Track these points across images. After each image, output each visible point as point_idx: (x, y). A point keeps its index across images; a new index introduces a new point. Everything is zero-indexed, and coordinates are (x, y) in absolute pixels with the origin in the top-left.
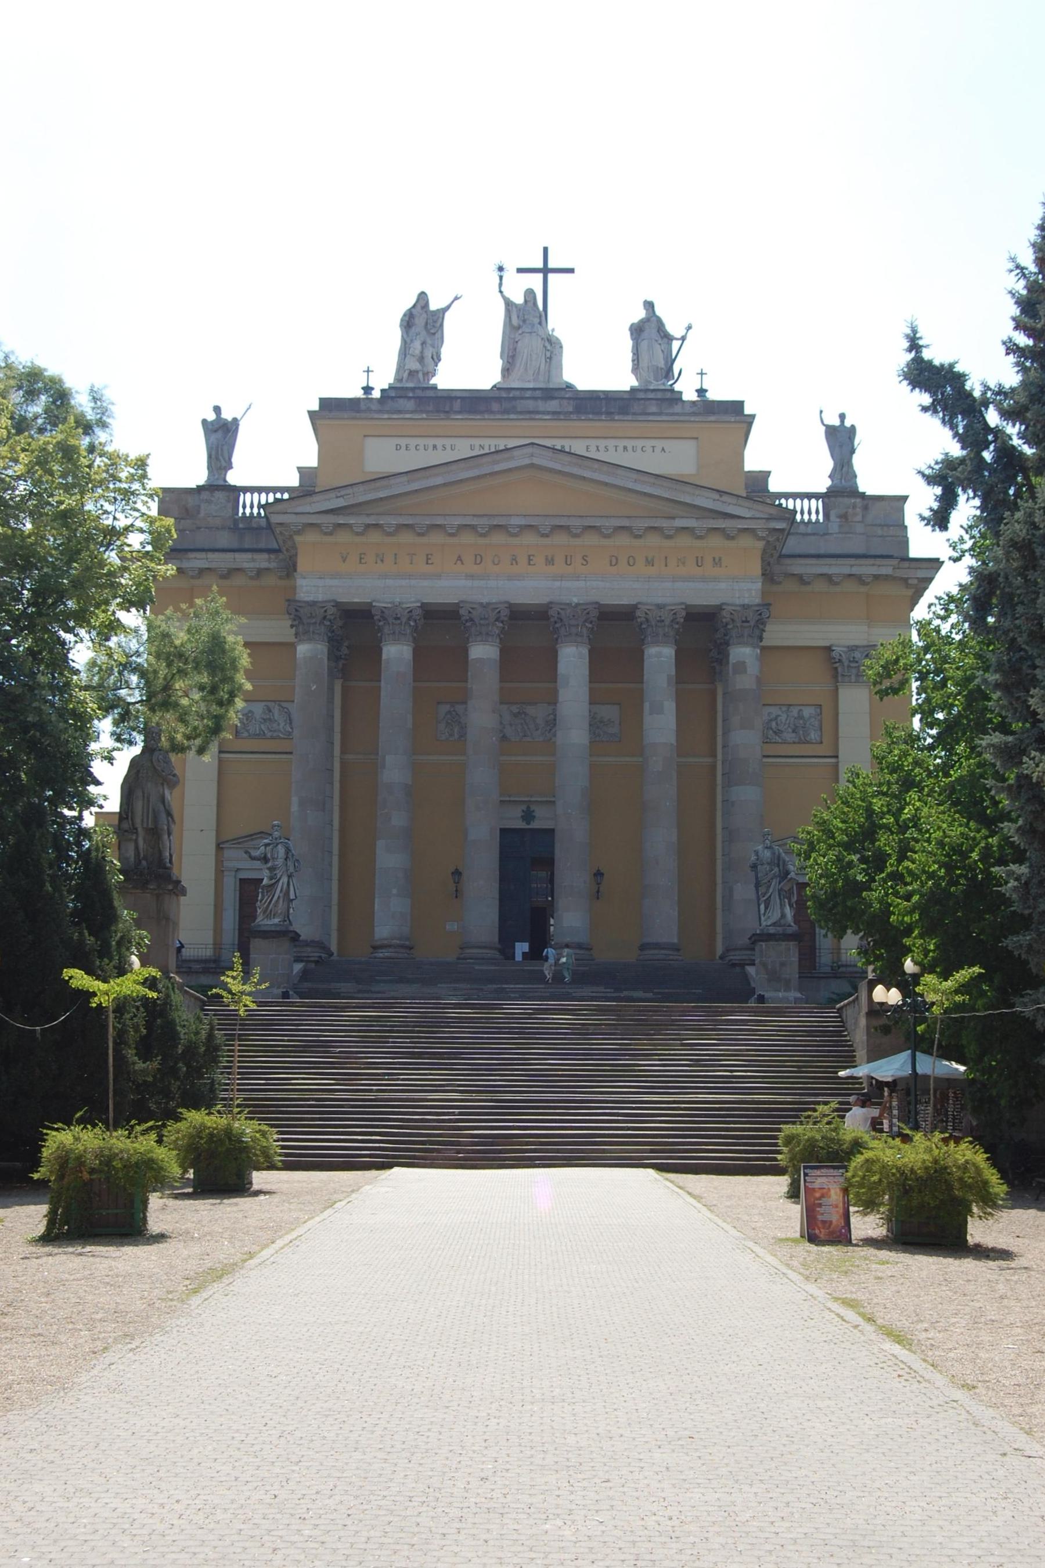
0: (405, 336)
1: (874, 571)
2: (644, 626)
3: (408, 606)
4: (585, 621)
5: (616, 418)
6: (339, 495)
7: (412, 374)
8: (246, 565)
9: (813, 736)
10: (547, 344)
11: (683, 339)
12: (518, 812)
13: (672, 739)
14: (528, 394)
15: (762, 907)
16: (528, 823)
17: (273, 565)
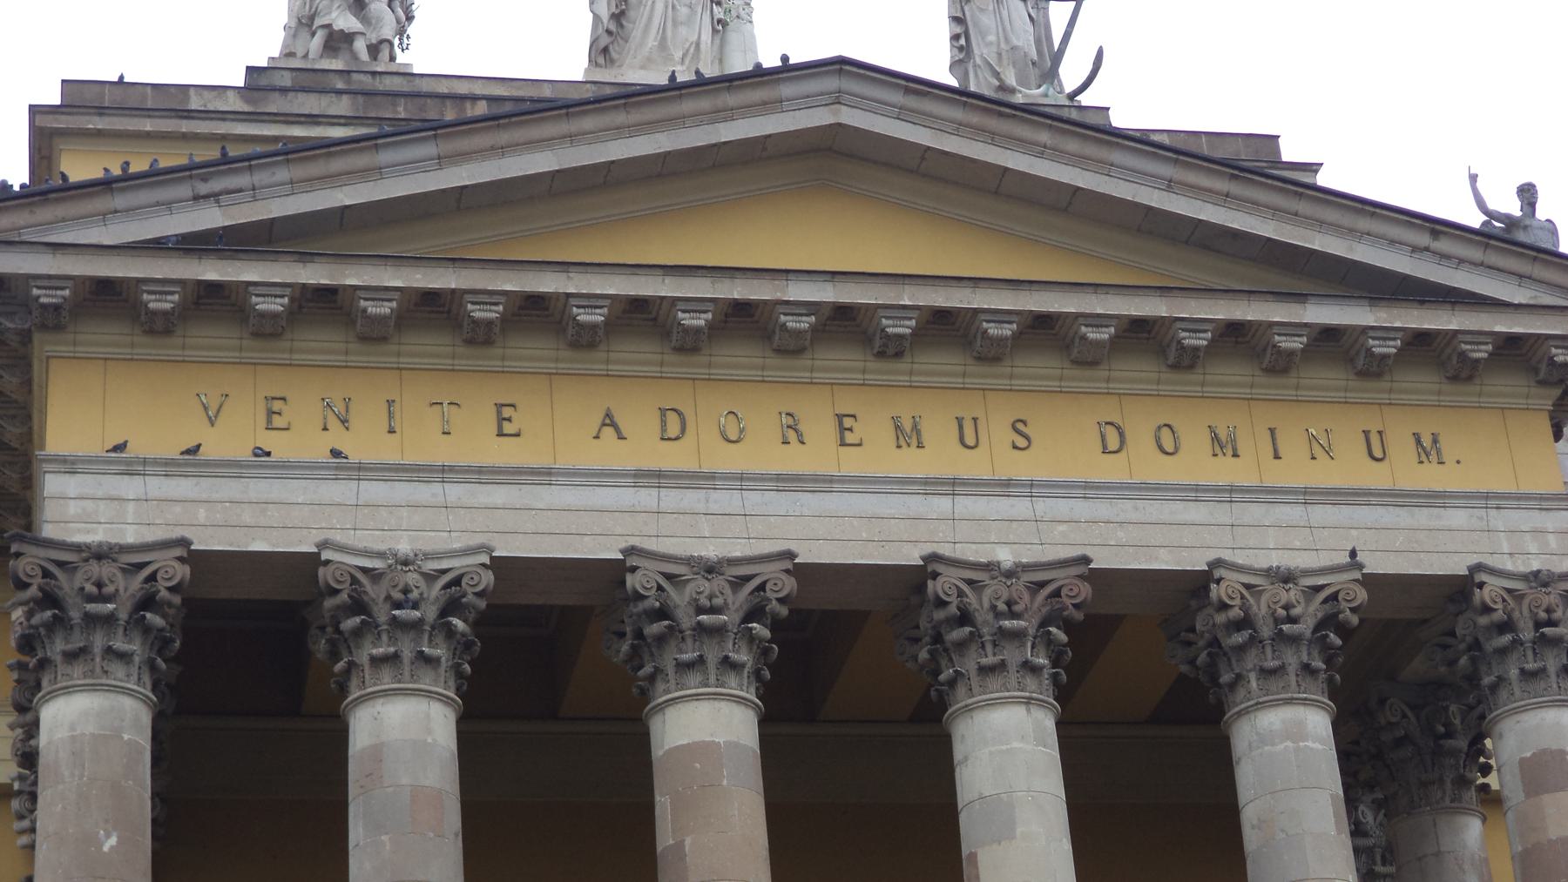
3: (444, 565)
6: (203, 188)
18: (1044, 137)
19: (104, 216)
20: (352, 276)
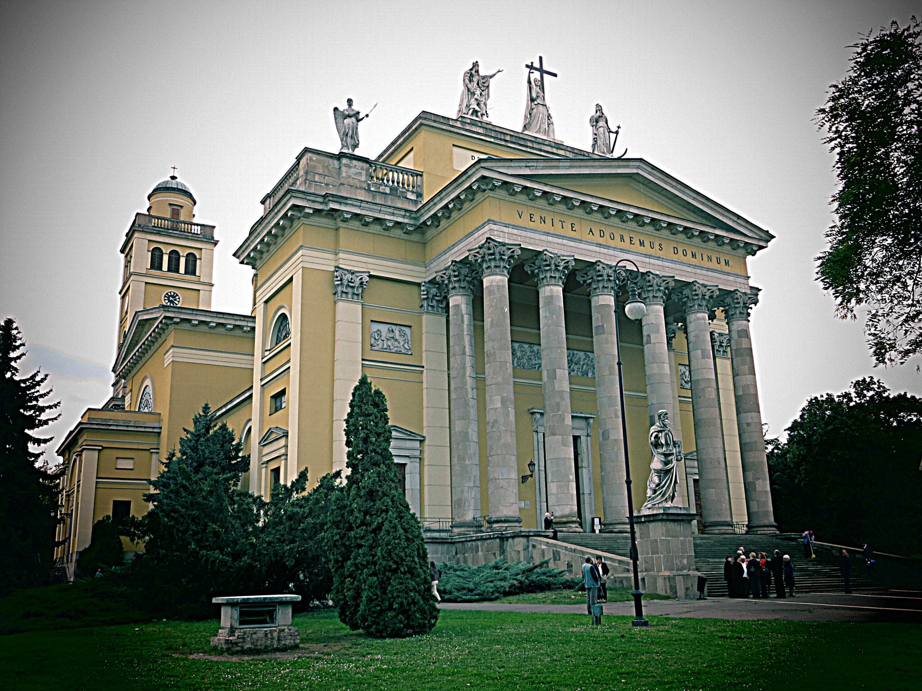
6: (528, 165)
11: (617, 133)
18: (674, 184)
19: (509, 167)
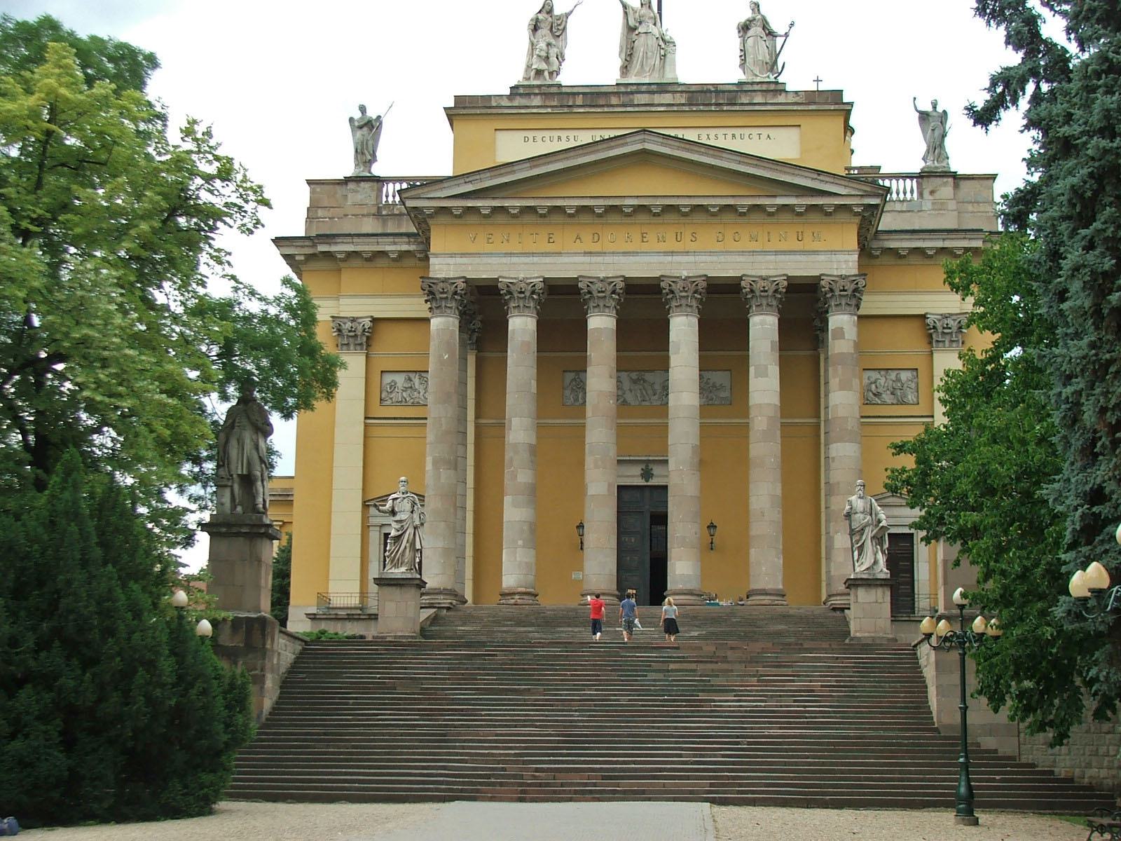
0: (532, 39)
1: (966, 244)
2: (749, 296)
3: (532, 281)
4: (695, 292)
5: (725, 108)
6: (467, 180)
7: (539, 73)
8: (388, 248)
9: (911, 397)
10: (661, 43)
11: (786, 35)
12: (637, 470)
13: (775, 400)
14: (644, 88)
15: (856, 553)
16: (647, 481)
17: (412, 248)
20: (506, 203)
